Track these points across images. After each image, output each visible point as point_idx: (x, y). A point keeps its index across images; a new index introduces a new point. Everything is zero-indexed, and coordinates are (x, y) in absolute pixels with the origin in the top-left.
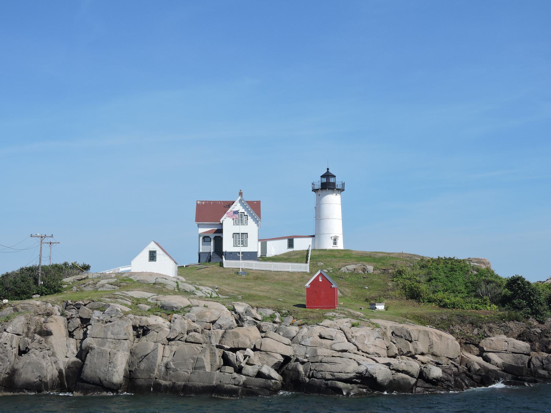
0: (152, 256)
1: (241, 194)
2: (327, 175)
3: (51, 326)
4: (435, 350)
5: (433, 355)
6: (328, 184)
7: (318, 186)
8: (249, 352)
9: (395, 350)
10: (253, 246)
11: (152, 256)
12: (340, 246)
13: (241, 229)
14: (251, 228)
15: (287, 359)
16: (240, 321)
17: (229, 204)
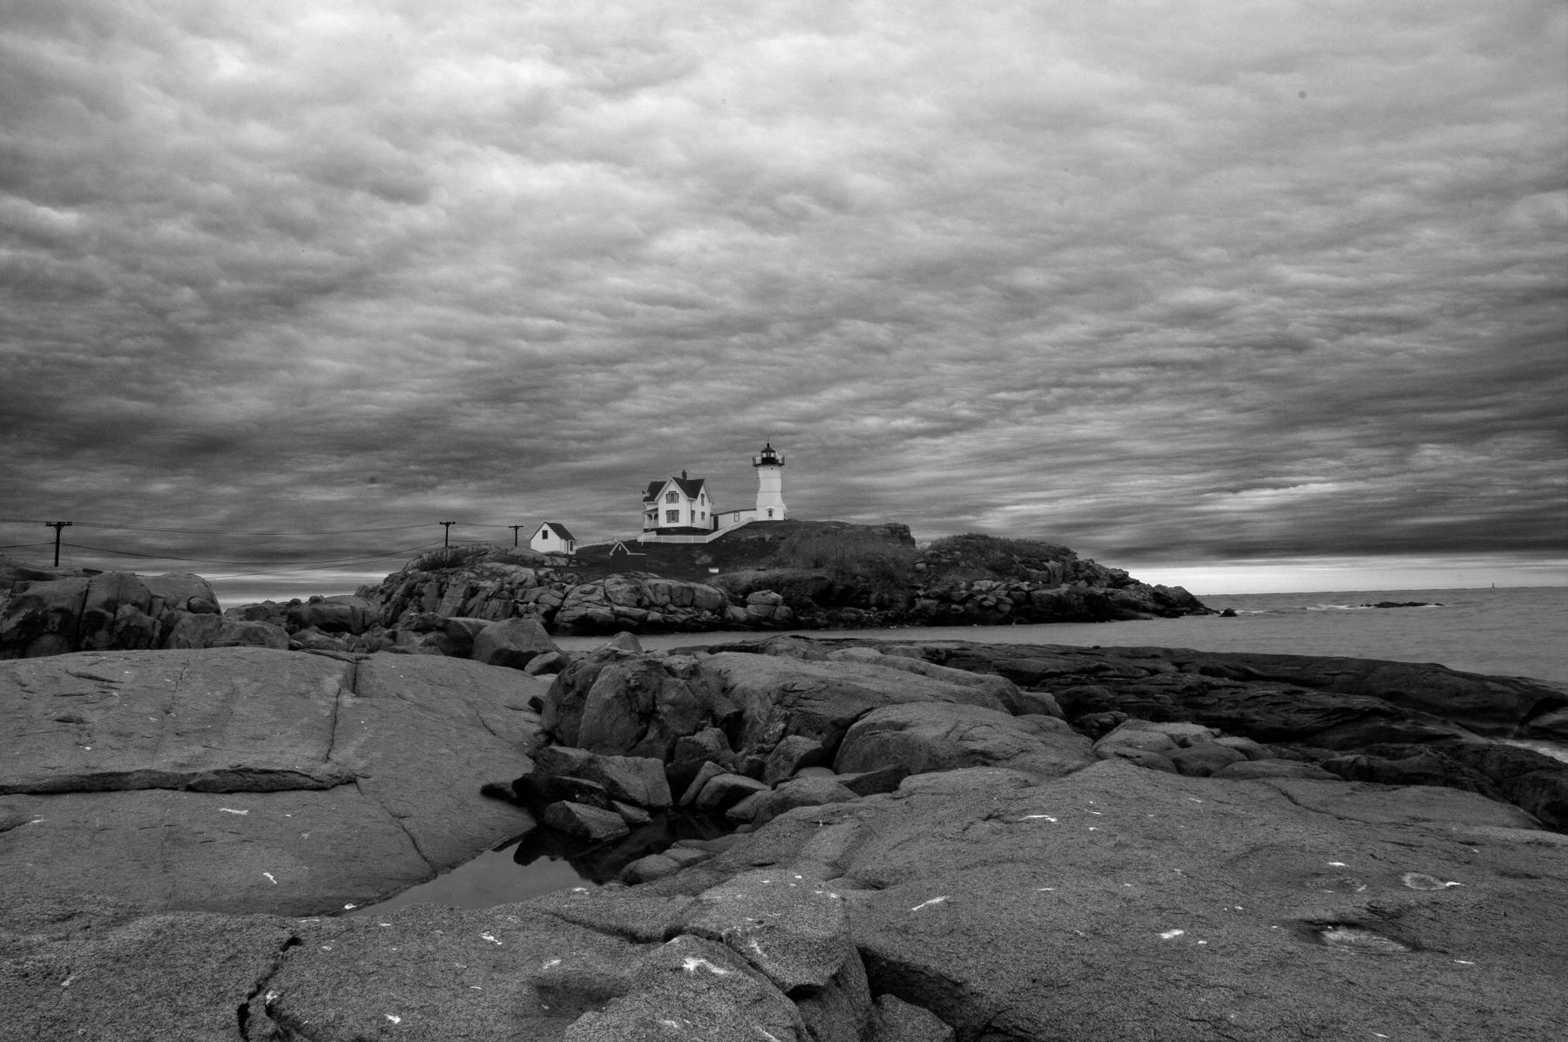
0: (545, 535)
1: (684, 474)
2: (768, 450)
3: (425, 590)
4: (697, 602)
5: (696, 607)
6: (769, 461)
7: (759, 460)
8: (532, 604)
9: (646, 602)
10: (684, 521)
11: (545, 535)
12: (778, 516)
13: (672, 507)
14: (683, 505)
15: (556, 609)
16: (540, 582)
17: (662, 484)
